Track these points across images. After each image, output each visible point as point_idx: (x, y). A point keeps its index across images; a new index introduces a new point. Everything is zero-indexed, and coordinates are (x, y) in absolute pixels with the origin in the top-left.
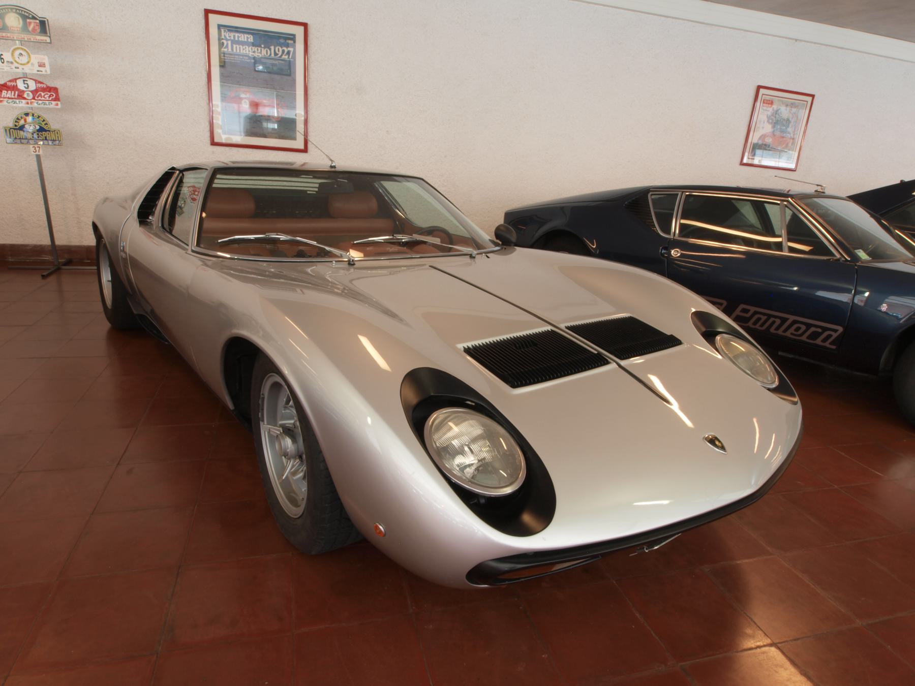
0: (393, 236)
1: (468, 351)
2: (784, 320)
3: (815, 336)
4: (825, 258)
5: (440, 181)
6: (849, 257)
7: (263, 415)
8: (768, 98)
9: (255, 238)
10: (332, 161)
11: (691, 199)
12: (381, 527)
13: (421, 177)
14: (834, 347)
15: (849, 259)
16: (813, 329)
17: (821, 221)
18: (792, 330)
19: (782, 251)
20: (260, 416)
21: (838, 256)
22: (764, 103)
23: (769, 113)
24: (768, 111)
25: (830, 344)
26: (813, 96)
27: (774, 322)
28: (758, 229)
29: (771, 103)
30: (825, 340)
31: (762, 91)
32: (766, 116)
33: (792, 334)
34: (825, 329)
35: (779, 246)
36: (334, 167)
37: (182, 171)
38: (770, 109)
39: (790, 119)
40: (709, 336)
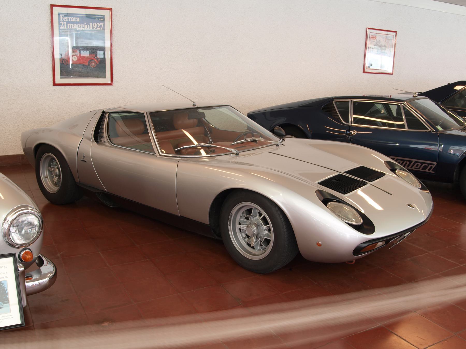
0: (245, 139)
1: (319, 183)
2: (411, 162)
3: (425, 168)
4: (424, 131)
5: (193, 96)
6: (434, 130)
7: (230, 223)
8: (373, 34)
9: (192, 146)
10: (193, 102)
11: (357, 104)
12: (321, 243)
13: (228, 105)
14: (434, 172)
15: (435, 131)
16: (424, 165)
17: (413, 108)
18: (415, 166)
19: (405, 129)
20: (229, 223)
21: (430, 129)
23: (375, 43)
24: (374, 41)
25: (432, 171)
26: (396, 32)
27: (406, 163)
28: (385, 114)
29: (375, 38)
30: (429, 170)
33: (415, 168)
34: (429, 164)
35: (402, 126)
36: (195, 105)
37: (110, 113)
38: (375, 41)
40: (393, 170)
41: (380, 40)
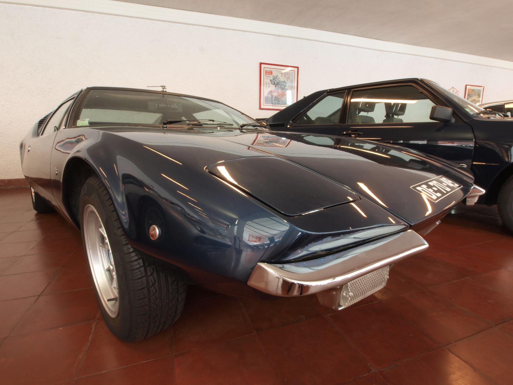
8: (268, 70)
22: (266, 72)
23: (271, 78)
24: (270, 77)
31: (263, 66)
32: (270, 80)
38: (272, 76)
39: (286, 81)
41: (277, 76)
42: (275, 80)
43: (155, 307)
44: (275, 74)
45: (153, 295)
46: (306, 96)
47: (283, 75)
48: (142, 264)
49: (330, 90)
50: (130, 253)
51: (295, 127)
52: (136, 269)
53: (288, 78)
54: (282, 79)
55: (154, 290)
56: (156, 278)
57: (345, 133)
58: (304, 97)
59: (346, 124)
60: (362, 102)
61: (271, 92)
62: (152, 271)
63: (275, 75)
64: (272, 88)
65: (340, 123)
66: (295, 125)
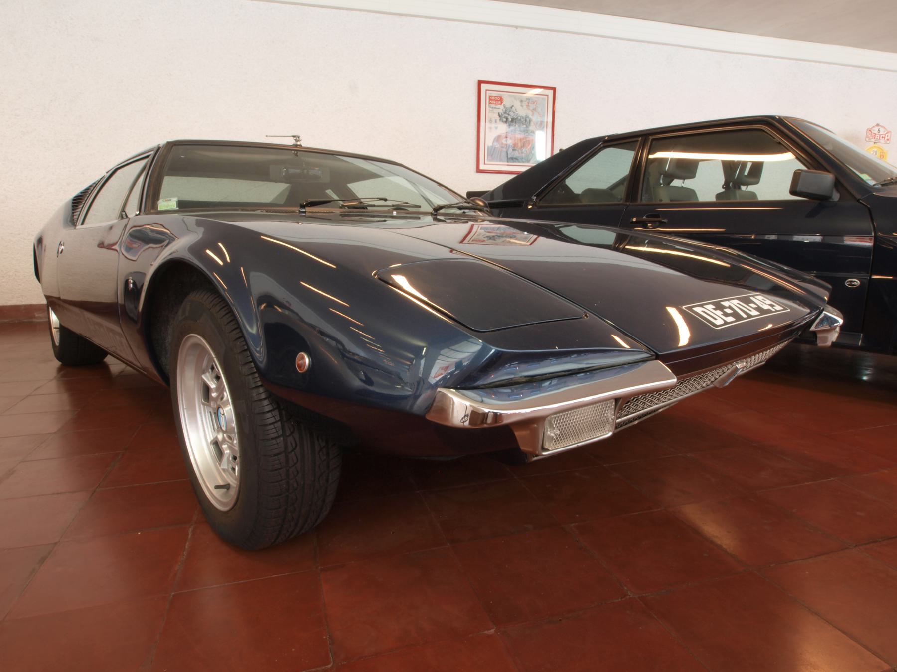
22: (490, 99)
24: (499, 108)
32: (497, 115)
38: (502, 106)
41: (513, 106)
42: (509, 115)
43: (295, 485)
44: (507, 102)
45: (293, 466)
46: (564, 148)
47: (525, 103)
48: (278, 418)
49: (609, 136)
50: (261, 400)
51: (541, 207)
52: (270, 424)
53: (535, 109)
54: (522, 112)
55: (294, 458)
56: (297, 440)
57: (635, 219)
58: (560, 150)
59: (639, 202)
60: (671, 159)
61: (498, 139)
62: (292, 430)
63: (508, 105)
64: (503, 128)
65: (627, 202)
66: (541, 204)
